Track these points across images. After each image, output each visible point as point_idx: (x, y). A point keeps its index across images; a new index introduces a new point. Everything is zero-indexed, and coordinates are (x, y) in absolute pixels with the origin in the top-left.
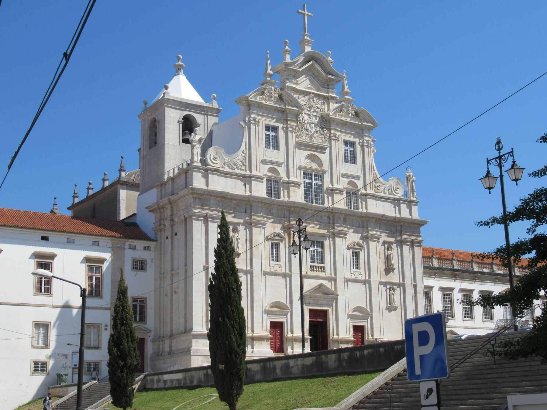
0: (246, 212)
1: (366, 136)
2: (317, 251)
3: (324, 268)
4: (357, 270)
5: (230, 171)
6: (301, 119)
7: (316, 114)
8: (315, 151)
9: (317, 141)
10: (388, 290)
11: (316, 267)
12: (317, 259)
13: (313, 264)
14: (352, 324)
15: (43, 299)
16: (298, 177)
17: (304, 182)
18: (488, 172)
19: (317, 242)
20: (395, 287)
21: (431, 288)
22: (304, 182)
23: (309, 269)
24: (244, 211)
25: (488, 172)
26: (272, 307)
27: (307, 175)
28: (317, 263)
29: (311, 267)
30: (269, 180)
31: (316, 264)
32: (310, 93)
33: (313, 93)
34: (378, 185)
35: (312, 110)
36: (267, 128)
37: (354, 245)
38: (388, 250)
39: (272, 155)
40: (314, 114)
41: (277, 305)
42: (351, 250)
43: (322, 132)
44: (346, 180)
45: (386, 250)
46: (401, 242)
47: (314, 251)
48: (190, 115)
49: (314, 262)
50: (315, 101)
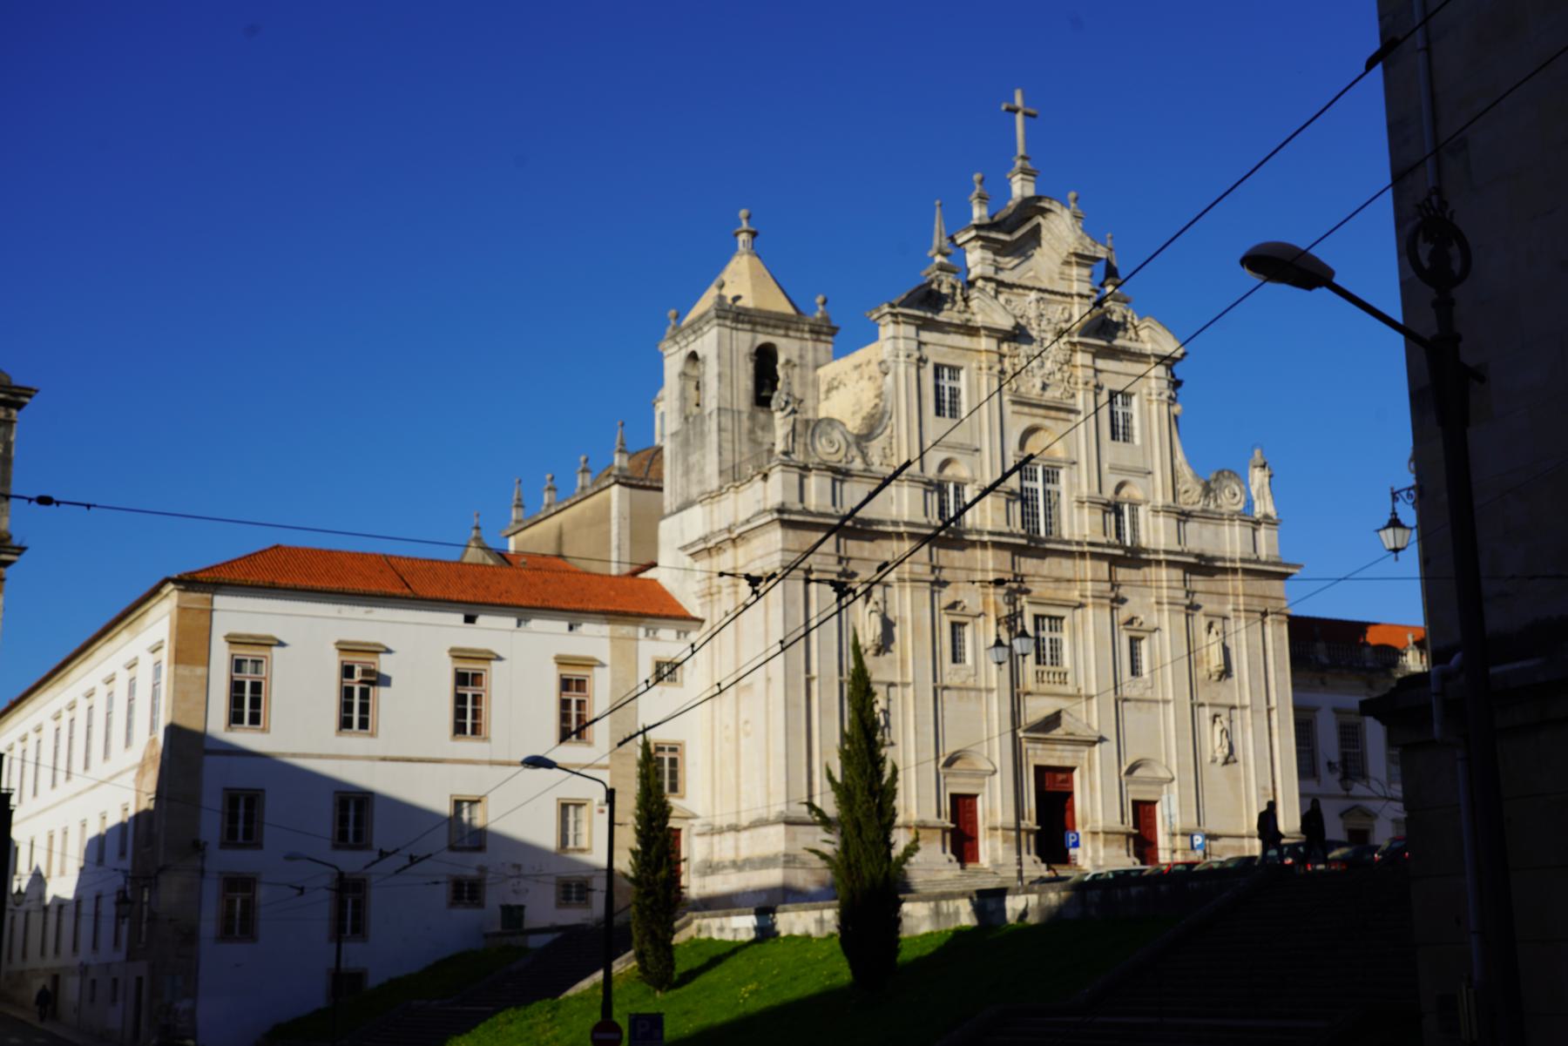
8: (1045, 417)
9: (1053, 394)
13: (1041, 668)
15: (467, 747)
18: (1394, 513)
19: (1050, 618)
21: (1316, 709)
25: (1394, 513)
33: (1040, 290)
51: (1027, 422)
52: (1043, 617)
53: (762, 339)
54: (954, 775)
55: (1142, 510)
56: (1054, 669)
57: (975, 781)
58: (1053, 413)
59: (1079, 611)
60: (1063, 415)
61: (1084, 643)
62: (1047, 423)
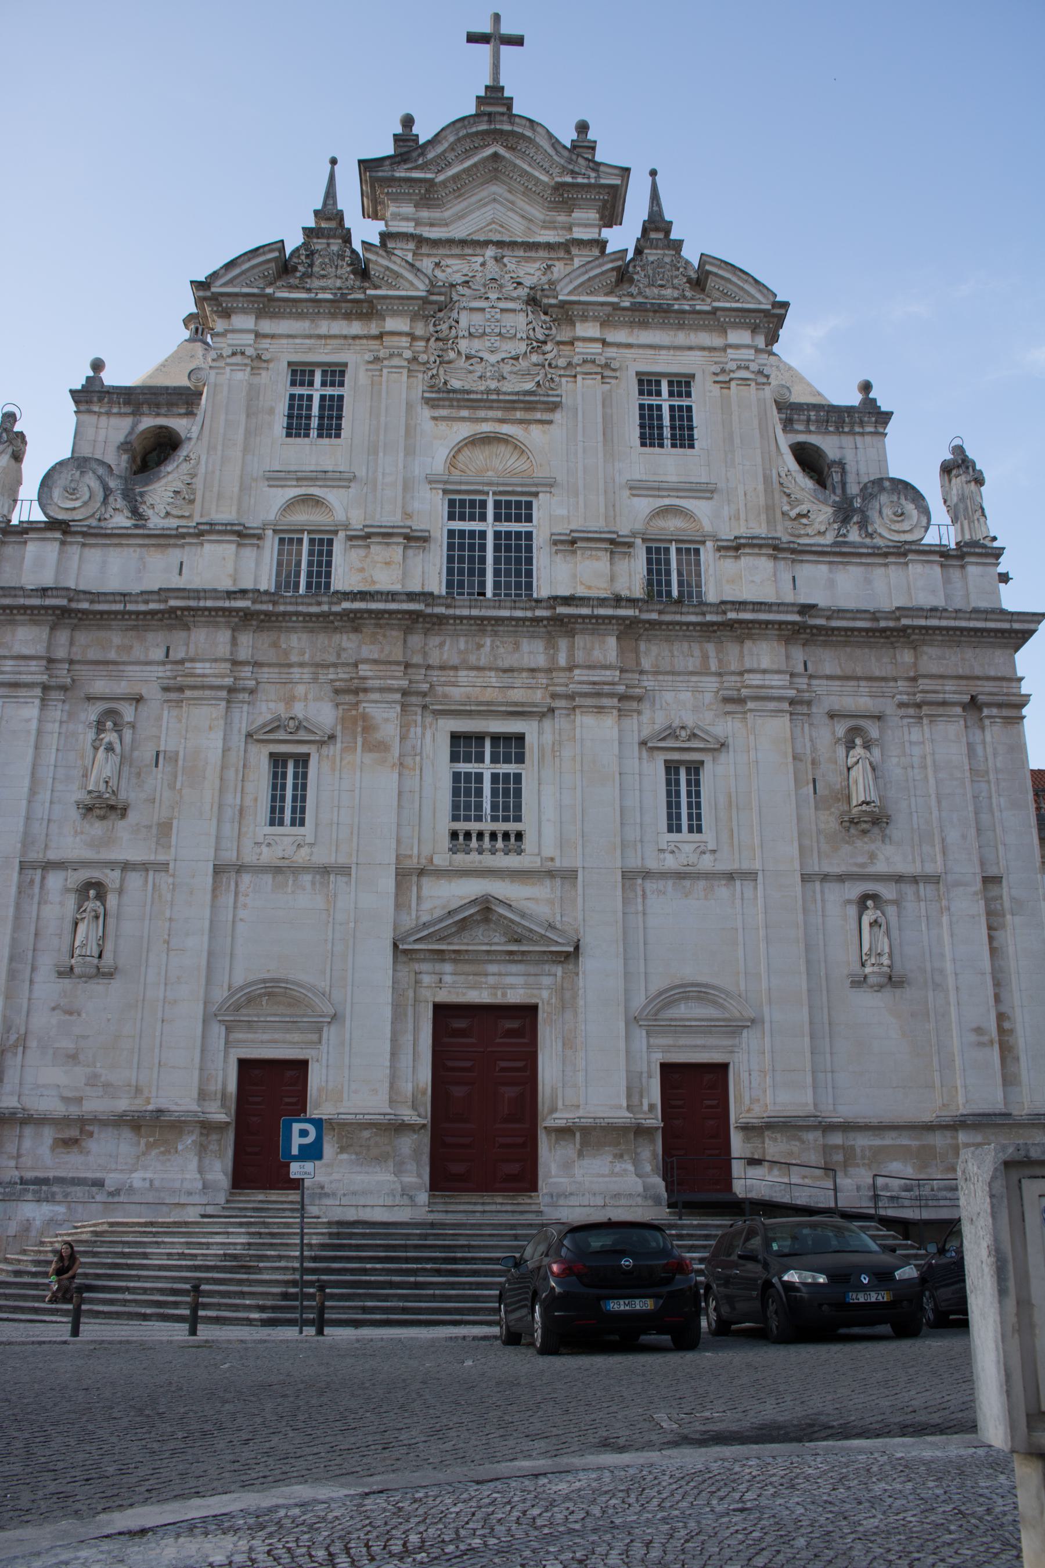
0: (167, 656)
1: (737, 347)
2: (495, 777)
3: (519, 836)
4: (695, 836)
5: (128, 523)
6: (444, 327)
7: (510, 305)
8: (502, 421)
10: (852, 911)
11: (480, 835)
12: (494, 807)
13: (461, 826)
14: (658, 1057)
16: (432, 514)
17: (451, 533)
19: (496, 738)
20: (887, 891)
22: (451, 533)
23: (445, 842)
24: (158, 654)
26: (251, 1000)
27: (462, 507)
28: (495, 819)
29: (454, 835)
30: (288, 540)
31: (487, 826)
32: (486, 243)
33: (500, 244)
34: (803, 509)
35: (493, 296)
36: (300, 374)
37: (677, 737)
38: (850, 746)
39: (312, 453)
40: (502, 305)
41: (272, 995)
42: (660, 758)
43: (535, 358)
44: (644, 505)
45: (841, 751)
46: (919, 706)
47: (479, 777)
48: (166, 428)
49: (479, 819)
50: (511, 266)
51: (464, 430)
52: (480, 738)
53: (148, 422)
54: (250, 1025)
55: (707, 554)
56: (501, 827)
57: (296, 1037)
58: (519, 415)
59: (547, 723)
60: (538, 416)
61: (584, 782)
62: (506, 429)
